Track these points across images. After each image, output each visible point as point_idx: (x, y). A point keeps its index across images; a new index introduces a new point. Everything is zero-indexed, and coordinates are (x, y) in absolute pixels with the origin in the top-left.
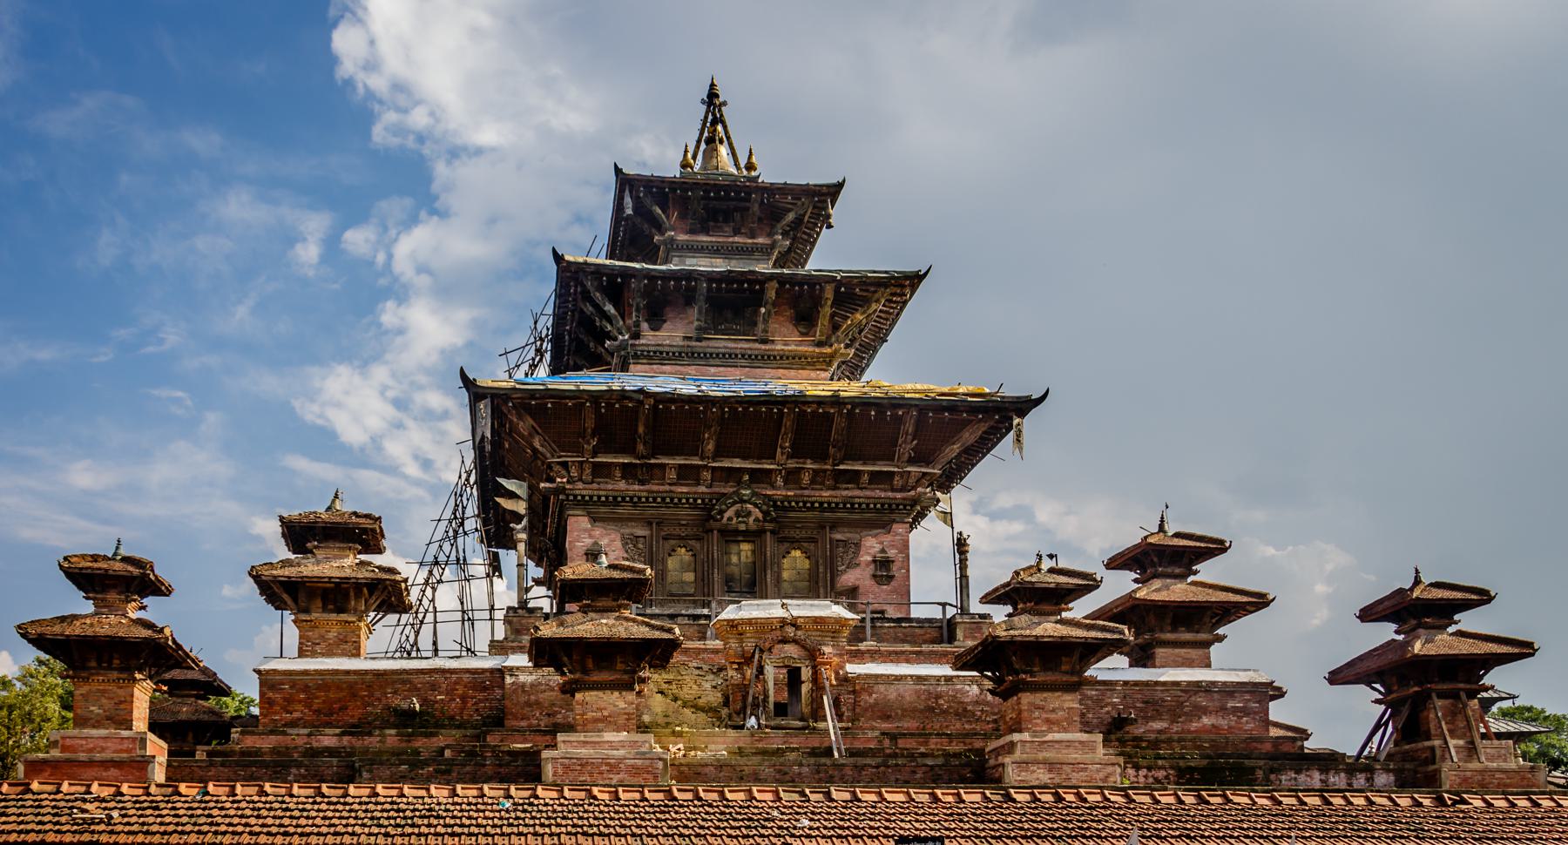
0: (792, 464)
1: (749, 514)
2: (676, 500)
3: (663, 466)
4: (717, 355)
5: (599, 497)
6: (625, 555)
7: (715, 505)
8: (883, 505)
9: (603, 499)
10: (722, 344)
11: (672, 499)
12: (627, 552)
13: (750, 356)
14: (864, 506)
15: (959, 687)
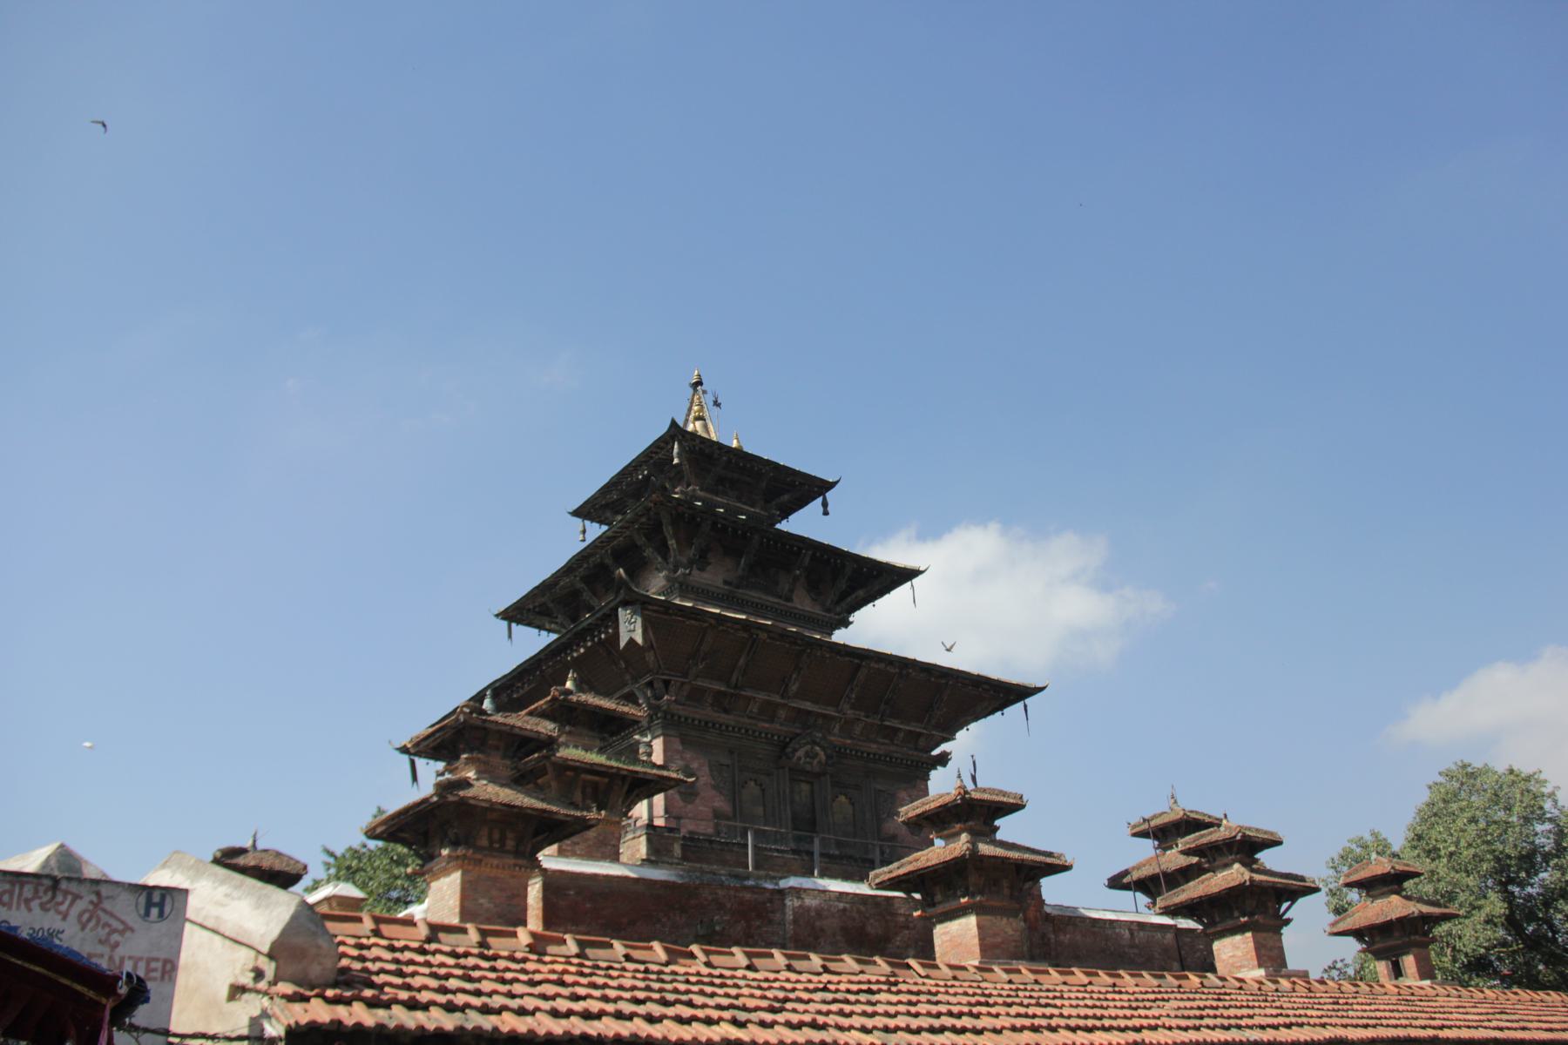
0: (850, 713)
1: (817, 755)
2: (757, 734)
3: (749, 699)
4: (753, 603)
5: (693, 720)
6: (713, 782)
7: (786, 745)
8: (912, 762)
9: (696, 722)
10: (753, 593)
11: (754, 732)
12: (714, 779)
13: (777, 610)
14: (899, 761)
15: (1117, 930)
